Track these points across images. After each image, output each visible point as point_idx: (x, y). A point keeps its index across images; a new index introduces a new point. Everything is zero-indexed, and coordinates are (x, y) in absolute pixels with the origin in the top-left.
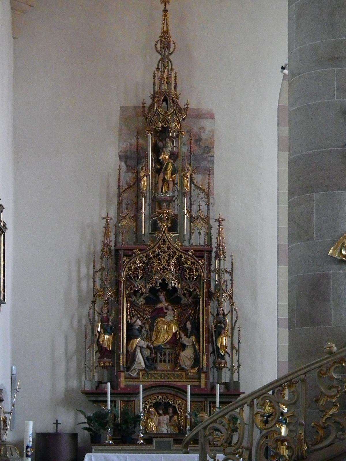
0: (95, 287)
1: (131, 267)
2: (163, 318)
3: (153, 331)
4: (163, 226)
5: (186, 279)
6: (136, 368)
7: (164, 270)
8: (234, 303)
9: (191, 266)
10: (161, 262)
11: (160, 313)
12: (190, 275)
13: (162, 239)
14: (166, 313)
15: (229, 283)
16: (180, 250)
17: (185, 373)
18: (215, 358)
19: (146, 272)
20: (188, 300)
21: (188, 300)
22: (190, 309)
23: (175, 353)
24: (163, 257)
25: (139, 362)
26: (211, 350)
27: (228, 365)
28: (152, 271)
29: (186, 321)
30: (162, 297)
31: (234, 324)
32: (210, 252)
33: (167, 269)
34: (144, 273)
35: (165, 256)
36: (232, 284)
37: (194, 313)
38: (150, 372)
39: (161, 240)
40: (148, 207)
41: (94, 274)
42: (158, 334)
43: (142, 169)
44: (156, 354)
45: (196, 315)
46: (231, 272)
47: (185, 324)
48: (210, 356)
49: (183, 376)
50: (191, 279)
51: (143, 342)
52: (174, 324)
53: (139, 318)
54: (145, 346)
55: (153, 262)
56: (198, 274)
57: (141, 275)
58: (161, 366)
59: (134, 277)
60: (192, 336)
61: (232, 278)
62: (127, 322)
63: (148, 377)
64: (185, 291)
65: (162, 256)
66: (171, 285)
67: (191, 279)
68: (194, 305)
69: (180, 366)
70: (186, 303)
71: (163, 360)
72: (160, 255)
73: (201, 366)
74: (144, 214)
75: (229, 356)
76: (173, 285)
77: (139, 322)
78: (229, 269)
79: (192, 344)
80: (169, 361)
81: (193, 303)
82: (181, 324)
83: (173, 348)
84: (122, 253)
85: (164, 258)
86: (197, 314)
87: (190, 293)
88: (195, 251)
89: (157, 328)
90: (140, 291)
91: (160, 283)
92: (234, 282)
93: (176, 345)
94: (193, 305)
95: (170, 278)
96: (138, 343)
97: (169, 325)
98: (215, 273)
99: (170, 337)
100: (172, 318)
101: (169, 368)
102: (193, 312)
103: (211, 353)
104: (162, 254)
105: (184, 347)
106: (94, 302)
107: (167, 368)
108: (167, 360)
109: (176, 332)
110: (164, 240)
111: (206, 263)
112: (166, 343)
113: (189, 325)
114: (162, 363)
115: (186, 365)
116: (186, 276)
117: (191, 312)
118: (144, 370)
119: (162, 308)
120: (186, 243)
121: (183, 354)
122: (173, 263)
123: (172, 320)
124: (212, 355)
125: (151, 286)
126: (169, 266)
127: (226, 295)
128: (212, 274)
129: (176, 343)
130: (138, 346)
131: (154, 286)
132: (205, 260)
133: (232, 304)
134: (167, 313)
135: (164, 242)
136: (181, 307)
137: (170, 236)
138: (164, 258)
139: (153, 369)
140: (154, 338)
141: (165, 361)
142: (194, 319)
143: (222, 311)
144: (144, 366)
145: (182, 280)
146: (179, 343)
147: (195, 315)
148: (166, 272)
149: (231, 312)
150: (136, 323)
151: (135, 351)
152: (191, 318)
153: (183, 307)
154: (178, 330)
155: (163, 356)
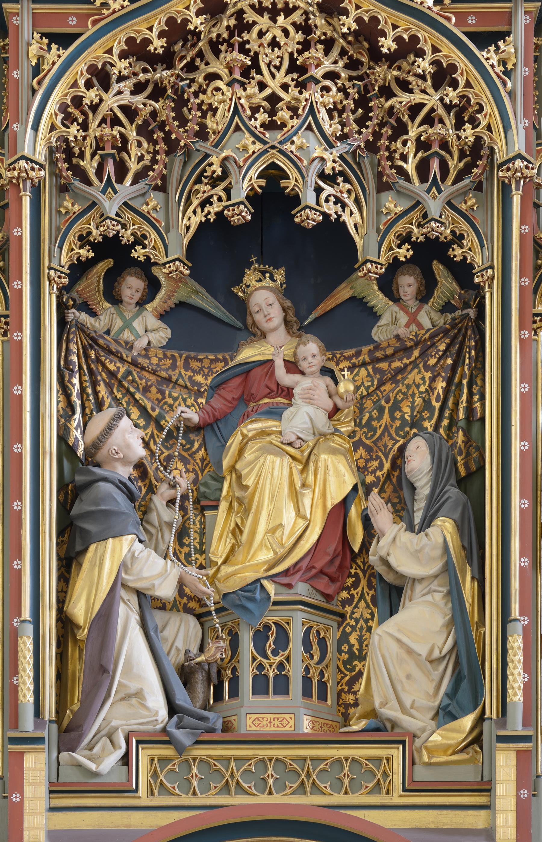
2: (270, 423)
11: (258, 391)
19: (168, 134)
22: (427, 368)
23: (340, 643)
24: (269, 37)
28: (203, 126)
30: (264, 295)
34: (155, 143)
35: (279, 35)
37: (447, 391)
42: (247, 512)
45: (456, 404)
49: (385, 774)
52: (333, 452)
55: (212, 77)
58: (256, 714)
59: (100, 172)
65: (261, 34)
69: (373, 714)
70: (402, 331)
71: (276, 677)
80: (307, 680)
83: (329, 608)
86: (464, 398)
89: (239, 477)
94: (442, 347)
100: (322, 421)
102: (440, 385)
105: (392, 594)
112: (286, 573)
114: (267, 693)
115: (408, 703)
117: (432, 389)
119: (268, 364)
125: (196, 221)
134: (296, 391)
136: (375, 360)
139: (212, 730)
141: (282, 686)
142: (449, 427)
147: (450, 403)
151: (105, 617)
153: (386, 358)
155: (275, 653)
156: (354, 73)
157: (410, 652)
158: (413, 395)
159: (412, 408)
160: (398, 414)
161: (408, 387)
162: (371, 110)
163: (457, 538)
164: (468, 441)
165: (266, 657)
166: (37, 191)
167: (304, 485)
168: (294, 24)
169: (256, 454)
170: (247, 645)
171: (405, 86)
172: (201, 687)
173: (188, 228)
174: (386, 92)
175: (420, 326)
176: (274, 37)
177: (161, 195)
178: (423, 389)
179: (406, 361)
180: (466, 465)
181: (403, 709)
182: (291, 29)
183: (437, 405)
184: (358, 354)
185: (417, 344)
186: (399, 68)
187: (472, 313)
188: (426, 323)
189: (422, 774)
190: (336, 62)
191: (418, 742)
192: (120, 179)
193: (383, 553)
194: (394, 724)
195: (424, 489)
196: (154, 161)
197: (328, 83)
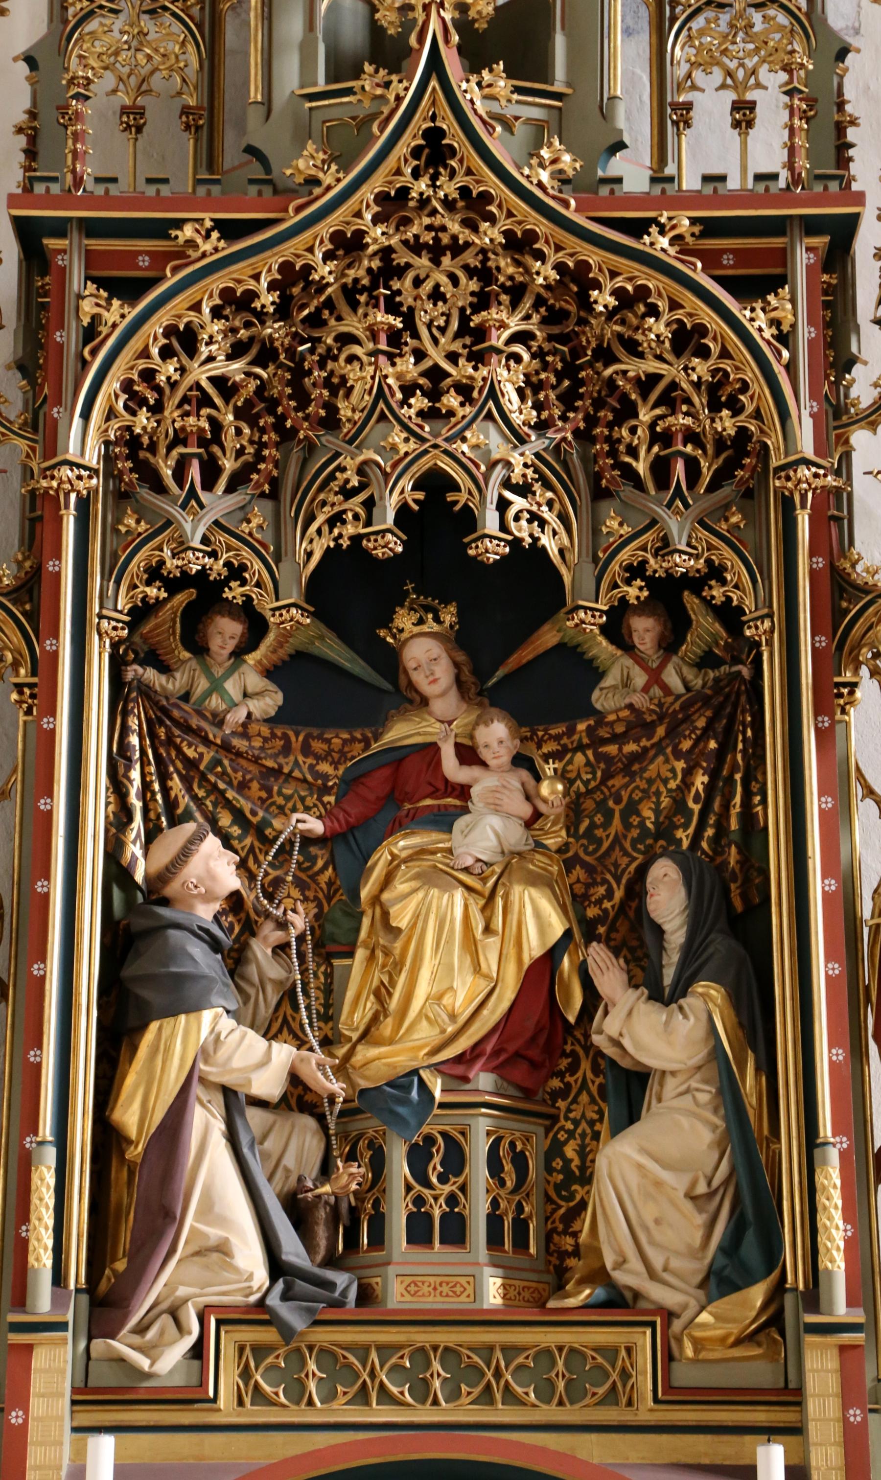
1: (148, 375)
3: (351, 954)
5: (629, 474)
6: (182, 1291)
7: (434, 395)
9: (671, 371)
10: (416, 335)
12: (663, 438)
13: (419, 123)
14: (463, 792)
16: (570, 214)
17: (644, 1339)
20: (655, 677)
21: (655, 677)
22: (678, 754)
24: (428, 286)
25: (214, 1233)
28: (332, 409)
30: (425, 651)
33: (464, 390)
37: (710, 788)
38: (324, 1336)
39: (402, 148)
42: (399, 965)
44: (378, 1164)
45: (726, 806)
47: (637, 889)
49: (625, 1375)
50: (680, 468)
51: (255, 1042)
52: (534, 880)
54: (268, 1084)
56: (742, 431)
57: (240, 452)
60: (700, 987)
62: (117, 872)
63: (298, 1393)
64: (628, 582)
65: (418, 282)
66: (504, 528)
73: (796, 1277)
76: (523, 530)
77: (215, 868)
79: (700, 1055)
80: (494, 1221)
82: (602, 890)
84: (70, 255)
85: (436, 290)
86: (738, 799)
87: (669, 596)
88: (710, 228)
89: (386, 915)
91: (403, 510)
93: (556, 1083)
94: (701, 723)
95: (492, 466)
96: (204, 1054)
99: (505, 1005)
101: (492, 1291)
102: (700, 780)
104: (423, 262)
105: (629, 1090)
107: (477, 1293)
109: (552, 957)
110: (434, 135)
111: (805, 334)
112: (459, 1059)
113: (668, 899)
116: (633, 452)
117: (686, 783)
118: (259, 1313)
119: (431, 750)
120: (632, 171)
121: (622, 1160)
122: (515, 338)
123: (513, 854)
126: (478, 358)
128: (859, 438)
129: (546, 1052)
130: (202, 1080)
131: (356, 539)
132: (795, 305)
135: (434, 153)
138: (437, 295)
140: (354, 1015)
141: (455, 1231)
144: (261, 1276)
145: (600, 494)
147: (716, 805)
148: (451, 413)
150: (194, 869)
152: (684, 837)
154: (568, 934)
155: (443, 1179)
156: (556, 330)
157: (658, 1184)
158: (658, 794)
159: (657, 811)
160: (635, 820)
161: (650, 782)
162: (582, 383)
163: (730, 1012)
164: (744, 862)
165: (428, 1185)
166: (84, 505)
167: (488, 930)
168: (466, 268)
169: (414, 884)
170: (399, 1167)
172: (330, 1232)
173: (309, 555)
176: (437, 286)
177: (269, 505)
178: (672, 785)
179: (644, 742)
180: (744, 896)
181: (652, 1274)
182: (460, 274)
183: (696, 808)
185: (661, 718)
186: (623, 322)
187: (745, 672)
189: (683, 1375)
190: (527, 317)
191: (677, 1325)
192: (209, 484)
193: (614, 1034)
194: (637, 1295)
195: (676, 935)
196: (259, 457)
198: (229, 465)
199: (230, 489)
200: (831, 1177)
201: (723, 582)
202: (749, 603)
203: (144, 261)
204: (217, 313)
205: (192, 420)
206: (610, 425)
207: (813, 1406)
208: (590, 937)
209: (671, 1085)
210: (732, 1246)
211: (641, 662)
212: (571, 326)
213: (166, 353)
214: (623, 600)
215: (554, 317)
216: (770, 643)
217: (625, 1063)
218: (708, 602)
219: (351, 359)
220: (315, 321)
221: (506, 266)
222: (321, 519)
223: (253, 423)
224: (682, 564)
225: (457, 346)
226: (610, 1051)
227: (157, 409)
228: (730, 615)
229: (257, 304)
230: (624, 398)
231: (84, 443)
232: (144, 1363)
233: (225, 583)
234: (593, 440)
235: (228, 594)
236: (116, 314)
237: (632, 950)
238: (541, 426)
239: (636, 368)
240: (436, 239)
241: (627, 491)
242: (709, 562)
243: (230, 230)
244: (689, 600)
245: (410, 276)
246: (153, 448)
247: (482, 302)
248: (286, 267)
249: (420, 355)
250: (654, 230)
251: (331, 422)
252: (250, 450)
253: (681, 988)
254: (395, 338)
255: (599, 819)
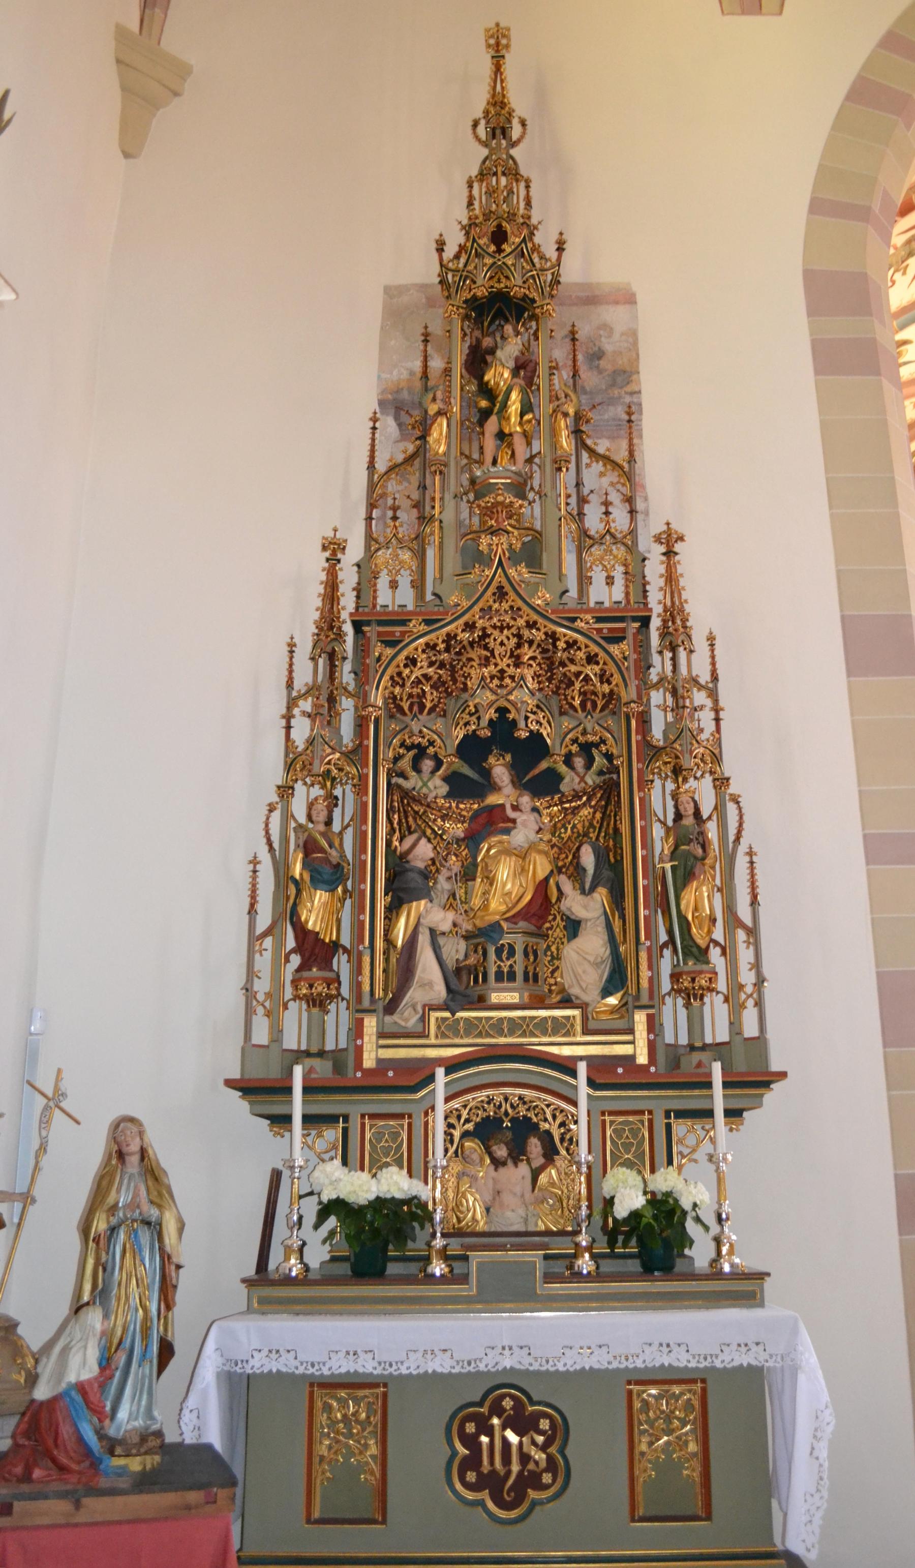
0: (290, 744)
1: (399, 674)
3: (474, 879)
4: (497, 545)
7: (502, 679)
8: (728, 779)
10: (494, 658)
13: (495, 584)
14: (514, 821)
15: (706, 718)
18: (678, 960)
20: (582, 779)
21: (582, 779)
26: (663, 937)
27: (722, 984)
28: (465, 684)
29: (577, 844)
30: (500, 771)
31: (731, 845)
32: (645, 621)
33: (512, 678)
36: (717, 720)
37: (602, 819)
40: (453, 502)
41: (288, 703)
43: (434, 399)
45: (608, 825)
46: (710, 685)
47: (576, 855)
48: (662, 956)
49: (572, 1025)
50: (589, 705)
52: (540, 852)
53: (426, 837)
56: (612, 691)
57: (433, 700)
61: (716, 701)
65: (495, 640)
66: (527, 726)
67: (589, 705)
68: (602, 795)
70: (577, 787)
71: (508, 972)
72: (489, 636)
74: (441, 522)
75: (724, 953)
76: (534, 727)
78: (705, 678)
80: (526, 974)
81: (596, 787)
82: (564, 856)
87: (587, 749)
90: (431, 750)
91: (491, 720)
92: (722, 714)
93: (547, 925)
94: (599, 795)
97: (523, 855)
98: (661, 690)
100: (533, 836)
102: (598, 815)
103: (665, 945)
104: (496, 633)
105: (573, 927)
106: (285, 791)
108: (519, 970)
109: (546, 880)
110: (500, 588)
112: (514, 916)
113: (588, 859)
116: (573, 698)
117: (594, 817)
119: (502, 806)
121: (571, 952)
124: (667, 953)
126: (517, 665)
127: (701, 750)
131: (474, 731)
133: (721, 783)
135: (501, 594)
137: (520, 573)
141: (512, 976)
143: (692, 804)
145: (562, 713)
146: (559, 918)
147: (605, 824)
149: (719, 809)
154: (552, 871)
155: (508, 959)
156: (545, 656)
159: (584, 828)
164: (615, 846)
165: (502, 961)
166: (377, 721)
168: (512, 634)
170: (492, 956)
171: (572, 661)
174: (563, 664)
175: (586, 783)
180: (615, 857)
182: (511, 637)
183: (598, 826)
184: (552, 799)
185: (584, 794)
188: (590, 782)
189: (592, 1025)
192: (421, 712)
193: (568, 905)
196: (439, 702)
197: (531, 662)
198: (429, 705)
199: (429, 713)
200: (643, 956)
201: (606, 744)
202: (615, 752)
203: (398, 634)
204: (423, 651)
205: (415, 689)
206: (565, 689)
207: (637, 1034)
208: (560, 871)
209: (589, 924)
210: (610, 979)
211: (577, 774)
212: (550, 653)
213: (406, 666)
214: (570, 751)
215: (545, 651)
216: (623, 766)
217: (573, 917)
218: (601, 751)
219: (472, 666)
220: (459, 654)
221: (526, 633)
222: (461, 723)
223: (437, 690)
224: (591, 738)
225: (510, 662)
226: (568, 913)
227: (403, 686)
228: (609, 757)
229: (438, 649)
230: (570, 679)
231: (377, 698)
232: (403, 1024)
233: (428, 747)
234: (559, 695)
235: (428, 751)
236: (389, 652)
237: (575, 877)
238: (540, 690)
239: (573, 668)
240: (502, 625)
241: (571, 712)
242: (601, 738)
243: (428, 622)
244: (595, 752)
245: (492, 637)
246: (401, 699)
247: (519, 646)
248: (448, 635)
249: (496, 665)
250: (579, 621)
251: (465, 689)
252: (436, 700)
253: (593, 889)
254: (487, 659)
255: (563, 830)
